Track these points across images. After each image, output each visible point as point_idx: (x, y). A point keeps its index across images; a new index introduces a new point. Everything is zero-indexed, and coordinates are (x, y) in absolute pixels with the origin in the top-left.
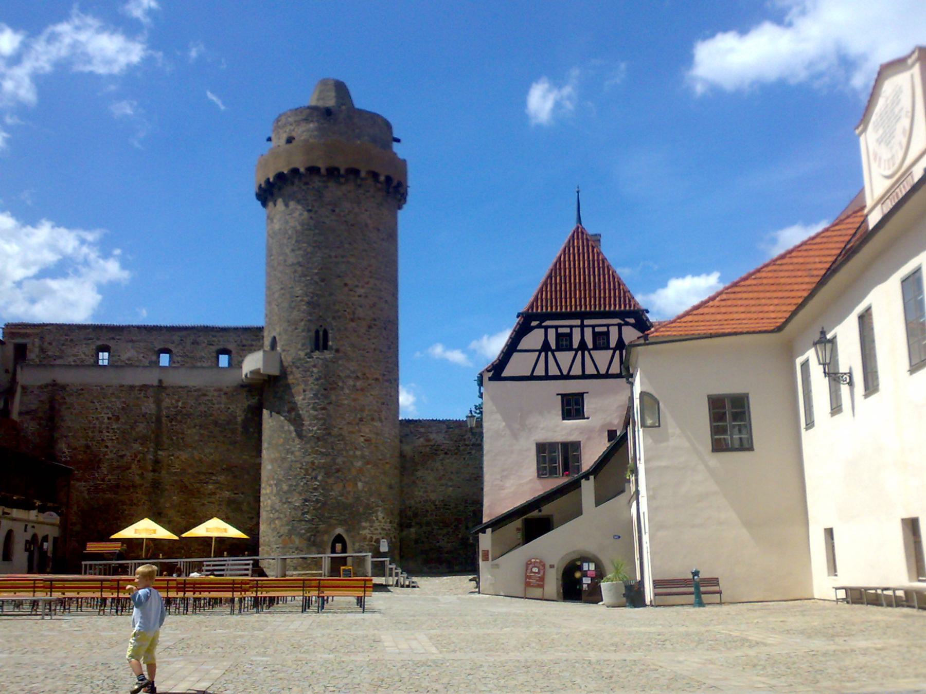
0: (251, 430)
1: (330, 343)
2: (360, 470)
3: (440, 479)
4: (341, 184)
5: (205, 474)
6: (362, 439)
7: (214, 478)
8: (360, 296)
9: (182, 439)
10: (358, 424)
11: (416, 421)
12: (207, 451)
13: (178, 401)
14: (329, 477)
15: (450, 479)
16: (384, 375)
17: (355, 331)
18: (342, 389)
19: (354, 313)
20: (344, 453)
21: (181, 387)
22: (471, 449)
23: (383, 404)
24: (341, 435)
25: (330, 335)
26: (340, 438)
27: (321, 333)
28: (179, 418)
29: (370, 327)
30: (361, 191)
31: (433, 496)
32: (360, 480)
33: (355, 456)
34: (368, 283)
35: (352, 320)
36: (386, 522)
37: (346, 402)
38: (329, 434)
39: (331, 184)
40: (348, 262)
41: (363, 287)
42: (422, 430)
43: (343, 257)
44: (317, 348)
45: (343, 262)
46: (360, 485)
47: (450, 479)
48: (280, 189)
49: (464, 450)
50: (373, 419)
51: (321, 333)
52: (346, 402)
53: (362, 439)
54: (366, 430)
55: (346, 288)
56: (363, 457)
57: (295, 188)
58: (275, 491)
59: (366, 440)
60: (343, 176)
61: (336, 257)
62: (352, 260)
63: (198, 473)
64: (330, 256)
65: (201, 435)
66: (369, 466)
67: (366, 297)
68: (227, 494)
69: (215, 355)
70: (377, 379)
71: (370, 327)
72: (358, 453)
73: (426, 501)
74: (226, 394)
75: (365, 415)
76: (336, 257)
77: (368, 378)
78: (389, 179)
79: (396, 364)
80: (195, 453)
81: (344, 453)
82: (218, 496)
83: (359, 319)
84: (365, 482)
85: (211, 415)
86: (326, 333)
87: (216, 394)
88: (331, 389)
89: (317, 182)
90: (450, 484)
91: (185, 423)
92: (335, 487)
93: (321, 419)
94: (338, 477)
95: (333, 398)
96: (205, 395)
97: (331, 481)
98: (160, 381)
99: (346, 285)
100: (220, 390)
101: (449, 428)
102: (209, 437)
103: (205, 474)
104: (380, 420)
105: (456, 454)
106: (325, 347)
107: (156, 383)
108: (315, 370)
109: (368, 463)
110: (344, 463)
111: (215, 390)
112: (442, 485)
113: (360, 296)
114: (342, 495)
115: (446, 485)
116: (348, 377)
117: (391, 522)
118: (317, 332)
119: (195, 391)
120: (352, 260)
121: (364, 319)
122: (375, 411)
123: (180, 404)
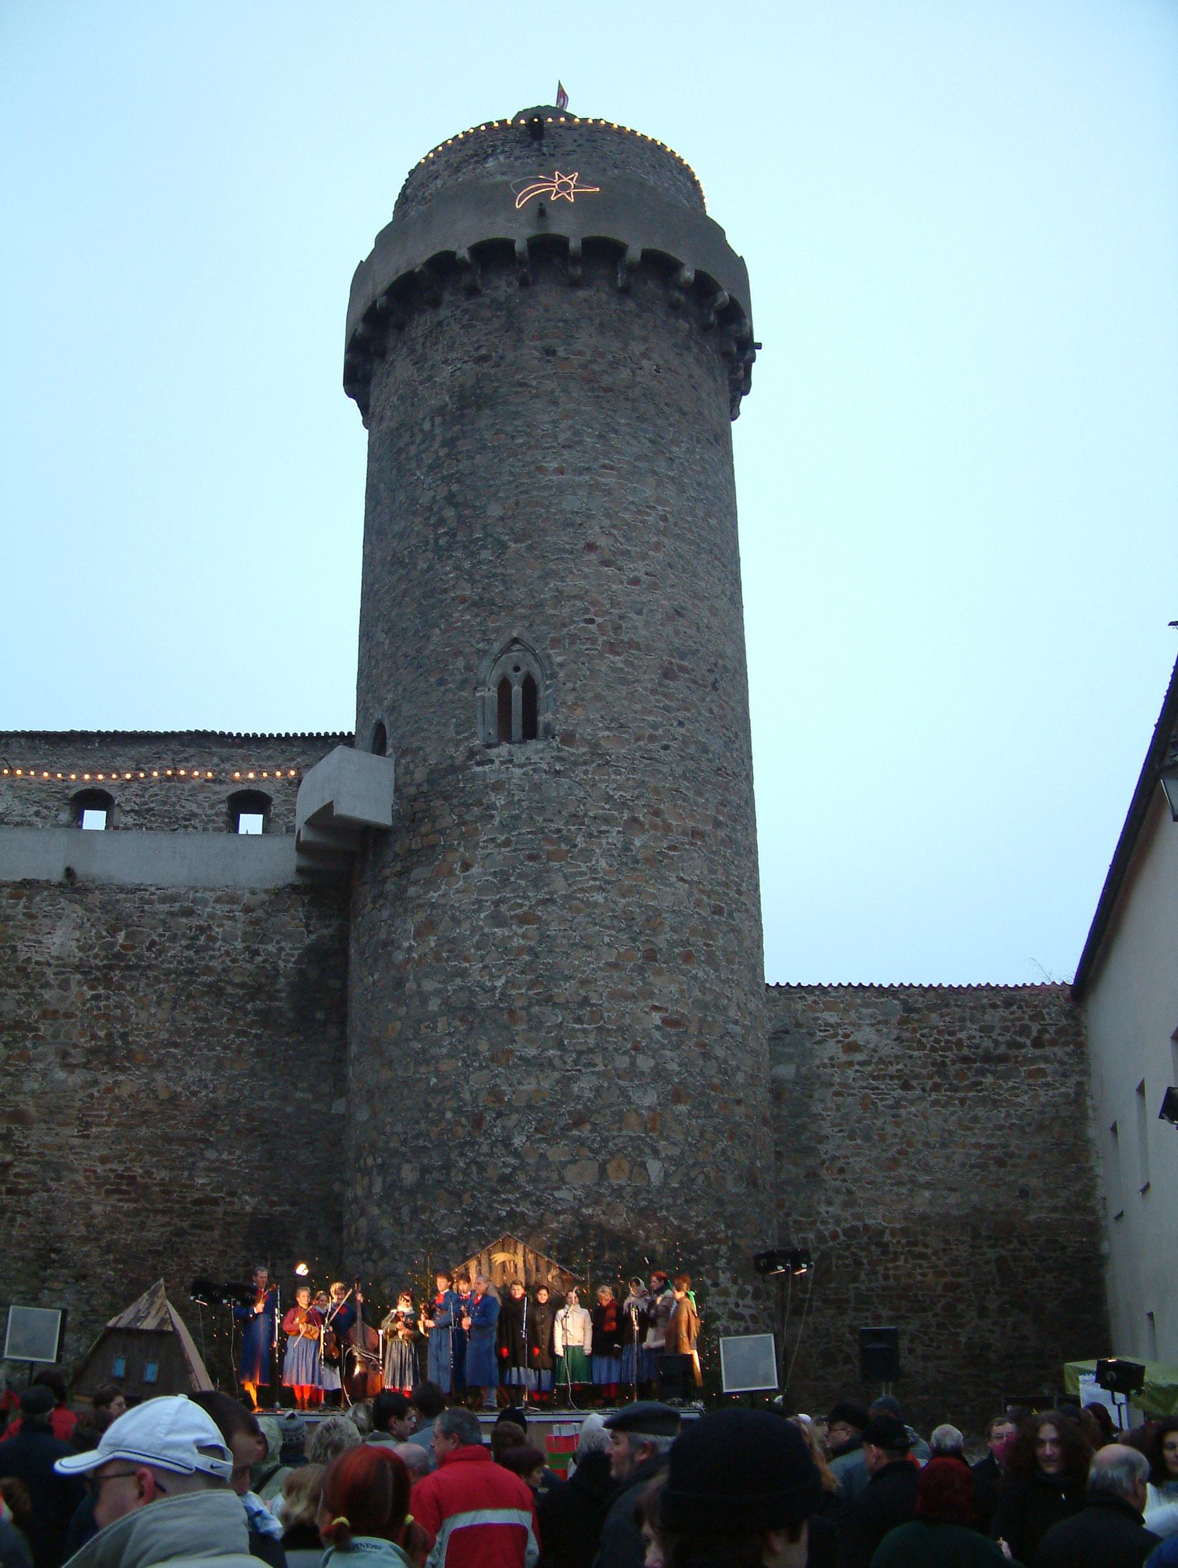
0: (319, 1015)
1: (544, 718)
2: (654, 1123)
3: (894, 1163)
4: (575, 284)
5: (182, 1141)
6: (656, 1018)
7: (211, 1154)
8: (635, 581)
9: (124, 1036)
10: (641, 969)
11: (810, 989)
12: (191, 1075)
13: (113, 931)
14: (551, 1140)
15: (927, 1168)
16: (717, 824)
17: (624, 681)
18: (587, 854)
19: (617, 629)
20: (598, 1060)
21: (121, 889)
22: (983, 1072)
23: (718, 911)
24: (585, 1002)
25: (542, 694)
26: (585, 1012)
27: (517, 689)
28: (116, 975)
29: (668, 674)
30: (630, 305)
31: (876, 1218)
32: (656, 1152)
33: (632, 1072)
34: (658, 547)
35: (612, 648)
36: (742, 1294)
37: (599, 898)
38: (549, 1000)
39: (548, 295)
40: (597, 485)
41: (644, 557)
42: (832, 1018)
43: (580, 472)
44: (505, 735)
45: (580, 485)
46: (655, 1168)
47: (927, 1168)
48: (401, 327)
49: (960, 1075)
50: (688, 957)
51: (517, 689)
52: (599, 898)
53: (656, 1018)
54: (667, 987)
55: (593, 556)
56: (659, 1073)
57: (444, 312)
58: (377, 1189)
59: (664, 1021)
60: (576, 260)
61: (560, 471)
62: (610, 480)
63: (167, 1139)
64: (540, 469)
65: (180, 1033)
66: (682, 1108)
67: (654, 586)
68: (249, 1203)
69: (224, 807)
70: (696, 833)
71: (668, 674)
72: (645, 1063)
73: (852, 1232)
74: (247, 910)
75: (661, 941)
76: (560, 471)
77: (668, 828)
78: (704, 286)
79: (749, 801)
80: (159, 1077)
81: (598, 1060)
82: (220, 1209)
83: (637, 646)
84: (670, 1158)
85: (208, 970)
86: (530, 687)
87: (221, 909)
88: (550, 856)
89: (503, 287)
90: (923, 1178)
91: (133, 992)
92: (570, 1173)
93: (521, 950)
94: (581, 1142)
95: (560, 886)
96: (188, 913)
97: (557, 1153)
98: (69, 873)
99: (591, 547)
100: (233, 900)
101: (908, 1009)
102: (199, 1032)
103: (182, 1141)
104: (711, 961)
105: (936, 1087)
106: (530, 731)
107: (57, 876)
108: (500, 800)
109: (677, 1098)
110: (598, 1091)
111: (218, 900)
112: (900, 1183)
113: (635, 581)
114: (597, 1202)
115: (913, 1180)
116: (607, 820)
117: (757, 1295)
118: (504, 687)
119: (163, 900)
120: (610, 480)
121: (649, 649)
122: (693, 931)
123: (121, 937)
